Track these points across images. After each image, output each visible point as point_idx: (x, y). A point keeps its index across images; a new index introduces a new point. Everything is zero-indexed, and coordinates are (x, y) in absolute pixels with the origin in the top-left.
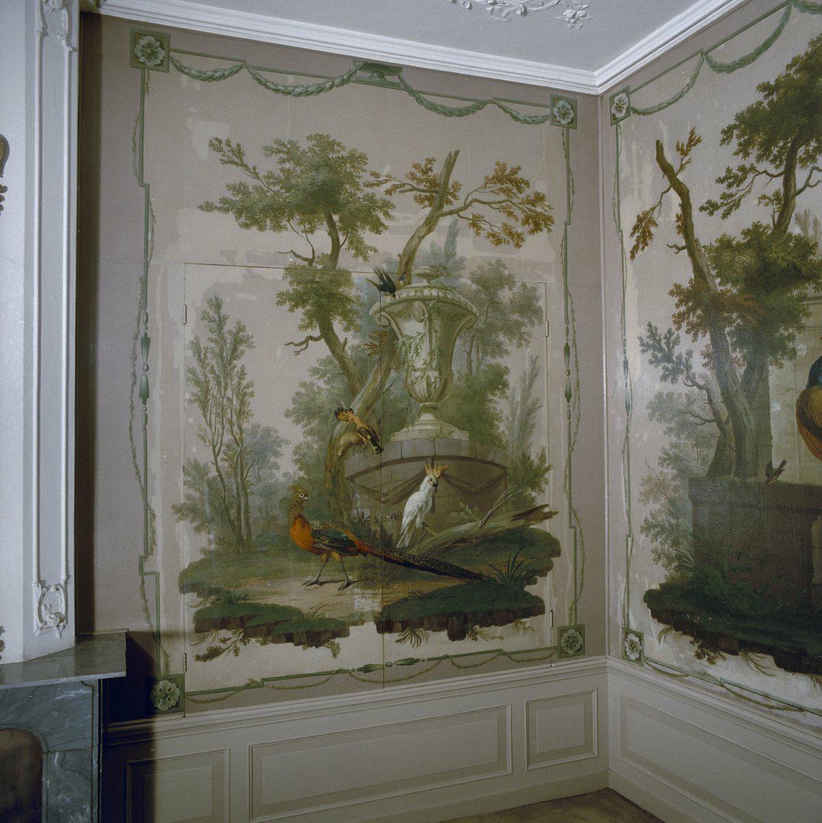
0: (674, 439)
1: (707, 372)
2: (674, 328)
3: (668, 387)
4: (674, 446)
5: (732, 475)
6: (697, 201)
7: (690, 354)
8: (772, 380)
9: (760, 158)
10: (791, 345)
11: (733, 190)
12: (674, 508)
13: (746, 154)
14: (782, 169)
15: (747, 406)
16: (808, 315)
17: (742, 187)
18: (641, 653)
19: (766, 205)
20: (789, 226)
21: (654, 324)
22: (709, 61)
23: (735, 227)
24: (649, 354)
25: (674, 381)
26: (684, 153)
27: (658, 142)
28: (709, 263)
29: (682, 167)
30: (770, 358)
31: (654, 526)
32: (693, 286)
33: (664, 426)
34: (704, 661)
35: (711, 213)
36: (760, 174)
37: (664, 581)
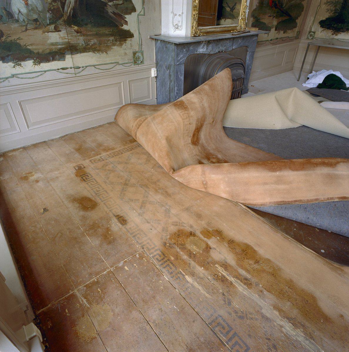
34: (334, 35)
37: (328, 17)
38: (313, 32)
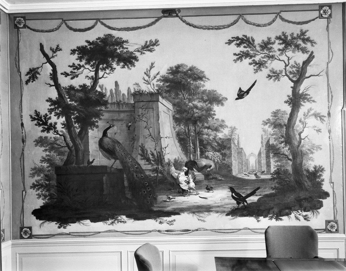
0: (48, 153)
1: (64, 130)
2: (48, 113)
3: (45, 134)
4: (47, 155)
5: (74, 164)
6: (59, 71)
7: (56, 123)
8: (90, 134)
9: (86, 64)
10: (97, 124)
11: (76, 71)
12: (48, 177)
13: (81, 61)
14: (94, 70)
15: (80, 142)
16: (103, 115)
17: (79, 71)
18: (31, 234)
19: (88, 79)
20: (97, 88)
21: (38, 111)
22: (66, 24)
23: (77, 83)
24: (35, 122)
25: (48, 132)
26: (54, 52)
27: (41, 44)
28: (65, 93)
29: (53, 57)
30: (89, 127)
31: (37, 186)
32: (57, 100)
33: (43, 148)
34: (62, 229)
35: (66, 76)
36: (86, 69)
38: (28, 228)
